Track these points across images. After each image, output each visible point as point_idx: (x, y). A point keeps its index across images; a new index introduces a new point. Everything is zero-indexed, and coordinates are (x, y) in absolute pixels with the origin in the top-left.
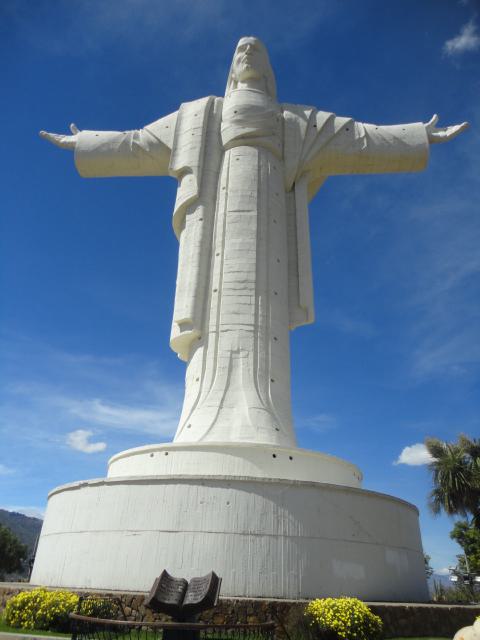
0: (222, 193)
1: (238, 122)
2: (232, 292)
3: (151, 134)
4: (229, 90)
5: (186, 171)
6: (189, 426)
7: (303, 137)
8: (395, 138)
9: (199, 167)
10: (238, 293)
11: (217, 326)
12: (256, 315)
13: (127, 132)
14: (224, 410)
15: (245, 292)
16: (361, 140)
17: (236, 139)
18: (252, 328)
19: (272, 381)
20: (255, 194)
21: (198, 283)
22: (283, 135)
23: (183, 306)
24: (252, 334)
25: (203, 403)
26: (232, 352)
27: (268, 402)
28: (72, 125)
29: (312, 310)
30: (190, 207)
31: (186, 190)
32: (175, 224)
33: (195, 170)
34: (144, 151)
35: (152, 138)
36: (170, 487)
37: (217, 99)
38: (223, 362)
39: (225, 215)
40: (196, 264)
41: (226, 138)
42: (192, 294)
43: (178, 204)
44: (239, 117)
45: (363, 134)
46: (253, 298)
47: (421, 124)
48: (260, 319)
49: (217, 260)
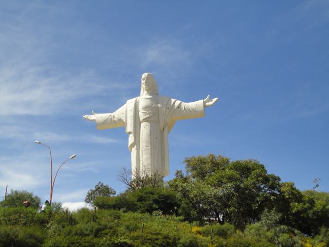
0: (141, 140)
5: (130, 133)
22: (158, 113)
30: (132, 145)
31: (131, 140)
33: (133, 132)
41: (141, 118)
43: (129, 144)
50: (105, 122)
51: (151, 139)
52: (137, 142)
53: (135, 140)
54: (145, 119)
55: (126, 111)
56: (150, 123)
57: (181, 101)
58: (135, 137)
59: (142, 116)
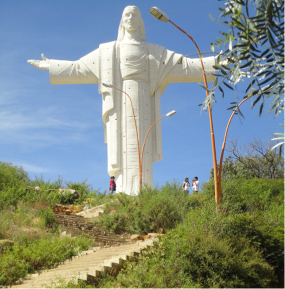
0: (124, 106)
2: (131, 153)
9: (113, 92)
10: (133, 153)
11: (127, 167)
15: (136, 153)
16: (185, 69)
17: (128, 76)
20: (138, 108)
23: (112, 159)
26: (133, 176)
28: (42, 55)
30: (110, 113)
31: (107, 104)
33: (111, 94)
34: (84, 76)
35: (88, 70)
38: (130, 180)
39: (126, 117)
40: (116, 141)
42: (116, 154)
45: (186, 67)
49: (124, 139)
50: (64, 74)
51: (139, 106)
52: (117, 108)
53: (115, 106)
54: (131, 75)
55: (100, 61)
56: (138, 82)
57: (173, 52)
59: (125, 71)
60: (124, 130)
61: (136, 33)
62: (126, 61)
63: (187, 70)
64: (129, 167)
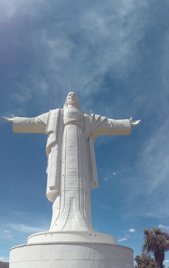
0: (64, 140)
1: (69, 117)
2: (69, 176)
3: (39, 119)
4: (65, 107)
5: (51, 132)
6: (56, 225)
7: (91, 123)
8: (121, 124)
9: (56, 131)
10: (72, 176)
12: (79, 185)
13: (31, 118)
14: (69, 219)
15: (74, 176)
16: (110, 124)
18: (78, 189)
19: (86, 209)
20: (77, 141)
21: (57, 173)
22: (85, 122)
23: (51, 182)
24: (78, 192)
25: (61, 216)
26: (71, 198)
27: (84, 216)
28: (12, 115)
29: (97, 183)
30: (52, 145)
31: (51, 139)
32: (47, 151)
33: (55, 132)
34: (36, 124)
35: (40, 121)
36: (57, 245)
37: (61, 109)
38: (67, 202)
40: (56, 166)
41: (65, 122)
42: (55, 177)
44: (69, 115)
45: (110, 123)
46: (78, 178)
47: (128, 120)
48: (80, 186)
49: (63, 164)
52: (59, 141)
53: (57, 140)
54: (71, 121)
58: (57, 137)
60: (63, 157)
61: (75, 104)
62: (68, 114)
63: (111, 125)
64: (68, 189)
